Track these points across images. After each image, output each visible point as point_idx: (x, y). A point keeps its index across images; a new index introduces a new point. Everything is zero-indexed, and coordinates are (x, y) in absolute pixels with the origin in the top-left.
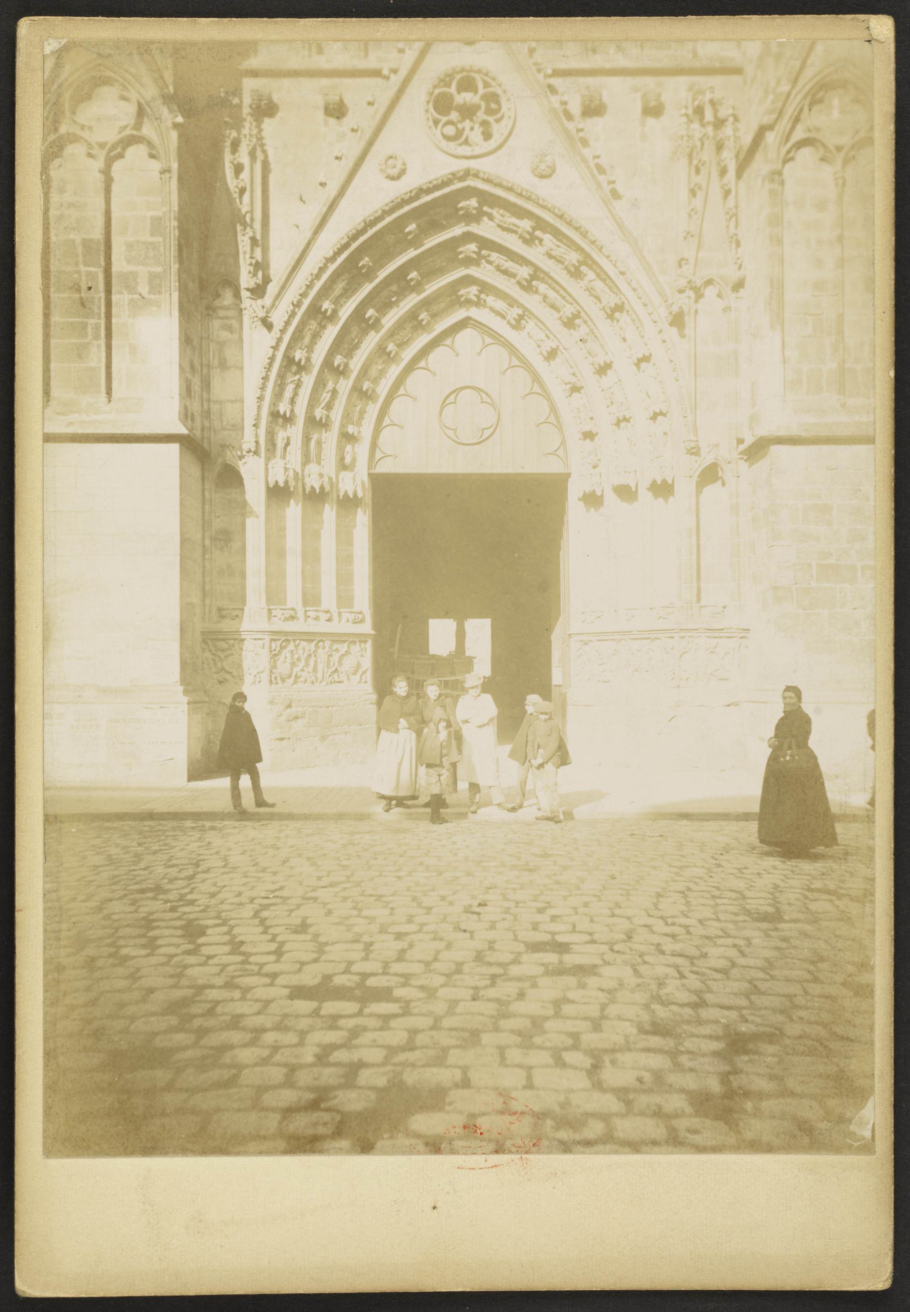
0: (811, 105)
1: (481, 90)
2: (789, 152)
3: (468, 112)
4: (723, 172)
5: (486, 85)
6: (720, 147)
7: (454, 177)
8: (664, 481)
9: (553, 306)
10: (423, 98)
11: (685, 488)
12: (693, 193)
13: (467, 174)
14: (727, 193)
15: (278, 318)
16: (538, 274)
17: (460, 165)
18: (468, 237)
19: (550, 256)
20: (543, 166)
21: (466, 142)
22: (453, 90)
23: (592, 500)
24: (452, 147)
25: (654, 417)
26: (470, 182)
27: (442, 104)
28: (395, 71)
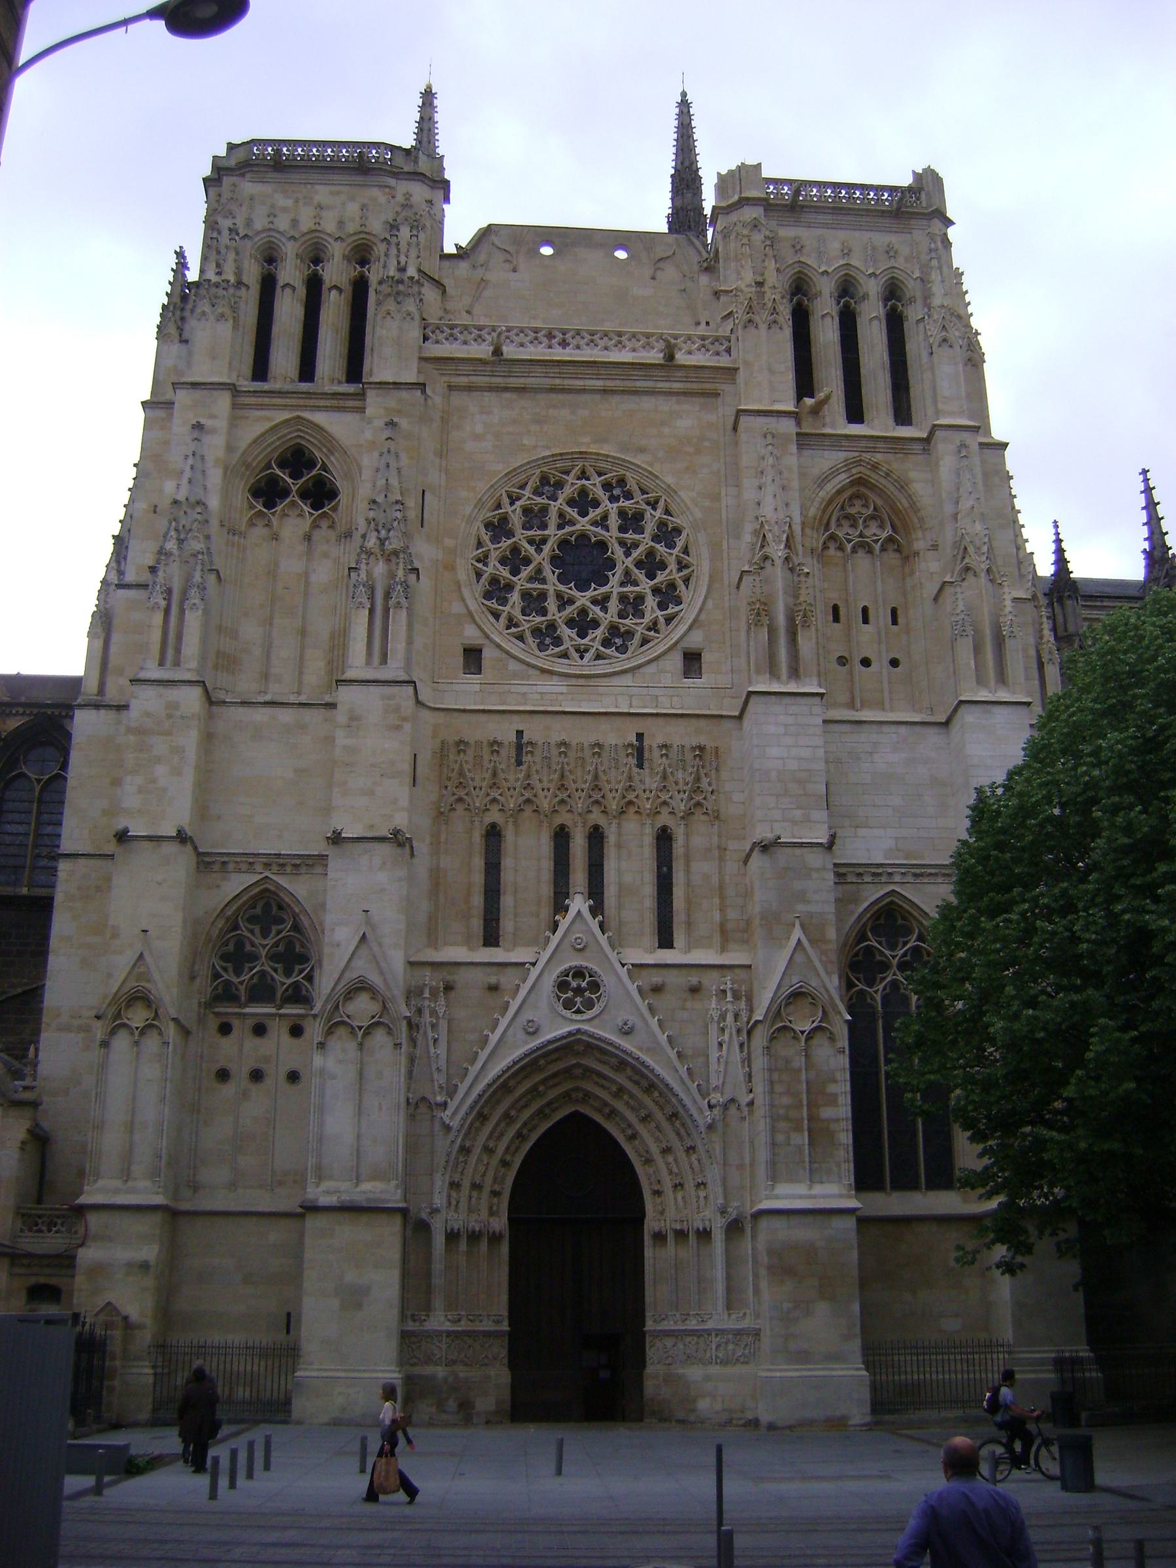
0: (787, 1004)
1: (588, 979)
2: (773, 1033)
3: (579, 991)
4: (739, 1031)
5: (590, 977)
6: (736, 1016)
7: (570, 1034)
8: (705, 1229)
9: (633, 1109)
10: (552, 983)
11: (718, 1236)
12: (720, 1044)
13: (579, 1031)
14: (741, 1045)
15: (455, 1123)
16: (622, 1089)
17: (573, 1027)
18: (578, 1065)
19: (630, 1079)
20: (626, 1027)
21: (578, 1012)
22: (570, 978)
23: (660, 1237)
24: (567, 1013)
25: (698, 1185)
26: (579, 1036)
27: (562, 986)
28: (534, 964)
